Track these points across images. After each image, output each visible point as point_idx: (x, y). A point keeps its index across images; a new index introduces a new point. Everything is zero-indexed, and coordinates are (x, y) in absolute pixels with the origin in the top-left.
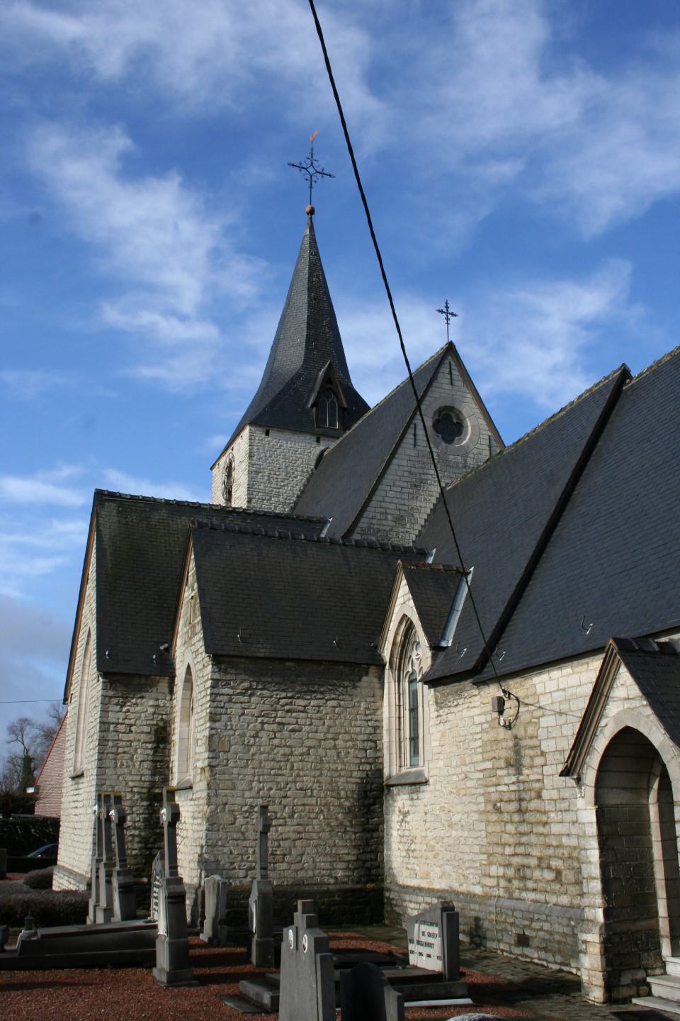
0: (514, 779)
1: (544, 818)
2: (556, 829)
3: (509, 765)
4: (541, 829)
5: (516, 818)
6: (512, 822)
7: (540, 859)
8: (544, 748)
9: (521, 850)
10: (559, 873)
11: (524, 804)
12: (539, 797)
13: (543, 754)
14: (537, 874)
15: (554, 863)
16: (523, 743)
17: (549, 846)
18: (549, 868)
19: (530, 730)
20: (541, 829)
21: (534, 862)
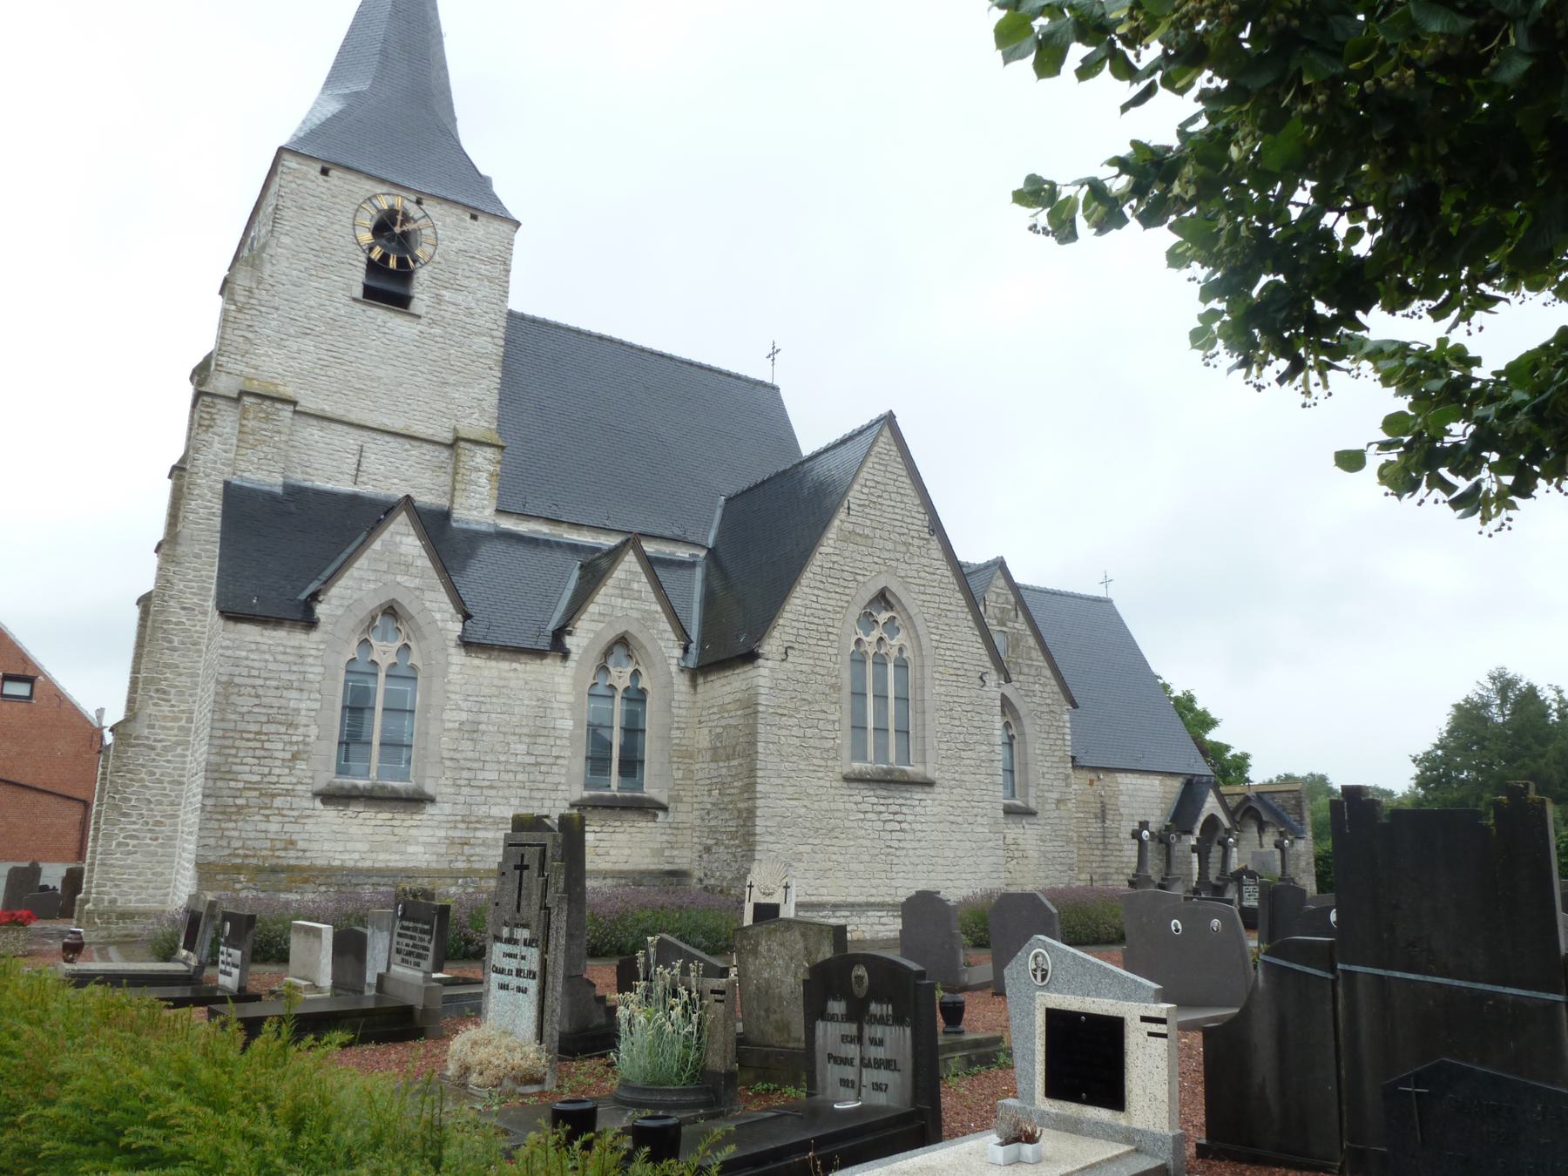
2: (1127, 853)
3: (1096, 817)
5: (1101, 847)
6: (1098, 849)
8: (1122, 810)
9: (1105, 864)
11: (1107, 840)
12: (1118, 837)
13: (1121, 815)
14: (1115, 877)
15: (1125, 871)
16: (1108, 807)
17: (1122, 862)
18: (1123, 873)
21: (1112, 871)
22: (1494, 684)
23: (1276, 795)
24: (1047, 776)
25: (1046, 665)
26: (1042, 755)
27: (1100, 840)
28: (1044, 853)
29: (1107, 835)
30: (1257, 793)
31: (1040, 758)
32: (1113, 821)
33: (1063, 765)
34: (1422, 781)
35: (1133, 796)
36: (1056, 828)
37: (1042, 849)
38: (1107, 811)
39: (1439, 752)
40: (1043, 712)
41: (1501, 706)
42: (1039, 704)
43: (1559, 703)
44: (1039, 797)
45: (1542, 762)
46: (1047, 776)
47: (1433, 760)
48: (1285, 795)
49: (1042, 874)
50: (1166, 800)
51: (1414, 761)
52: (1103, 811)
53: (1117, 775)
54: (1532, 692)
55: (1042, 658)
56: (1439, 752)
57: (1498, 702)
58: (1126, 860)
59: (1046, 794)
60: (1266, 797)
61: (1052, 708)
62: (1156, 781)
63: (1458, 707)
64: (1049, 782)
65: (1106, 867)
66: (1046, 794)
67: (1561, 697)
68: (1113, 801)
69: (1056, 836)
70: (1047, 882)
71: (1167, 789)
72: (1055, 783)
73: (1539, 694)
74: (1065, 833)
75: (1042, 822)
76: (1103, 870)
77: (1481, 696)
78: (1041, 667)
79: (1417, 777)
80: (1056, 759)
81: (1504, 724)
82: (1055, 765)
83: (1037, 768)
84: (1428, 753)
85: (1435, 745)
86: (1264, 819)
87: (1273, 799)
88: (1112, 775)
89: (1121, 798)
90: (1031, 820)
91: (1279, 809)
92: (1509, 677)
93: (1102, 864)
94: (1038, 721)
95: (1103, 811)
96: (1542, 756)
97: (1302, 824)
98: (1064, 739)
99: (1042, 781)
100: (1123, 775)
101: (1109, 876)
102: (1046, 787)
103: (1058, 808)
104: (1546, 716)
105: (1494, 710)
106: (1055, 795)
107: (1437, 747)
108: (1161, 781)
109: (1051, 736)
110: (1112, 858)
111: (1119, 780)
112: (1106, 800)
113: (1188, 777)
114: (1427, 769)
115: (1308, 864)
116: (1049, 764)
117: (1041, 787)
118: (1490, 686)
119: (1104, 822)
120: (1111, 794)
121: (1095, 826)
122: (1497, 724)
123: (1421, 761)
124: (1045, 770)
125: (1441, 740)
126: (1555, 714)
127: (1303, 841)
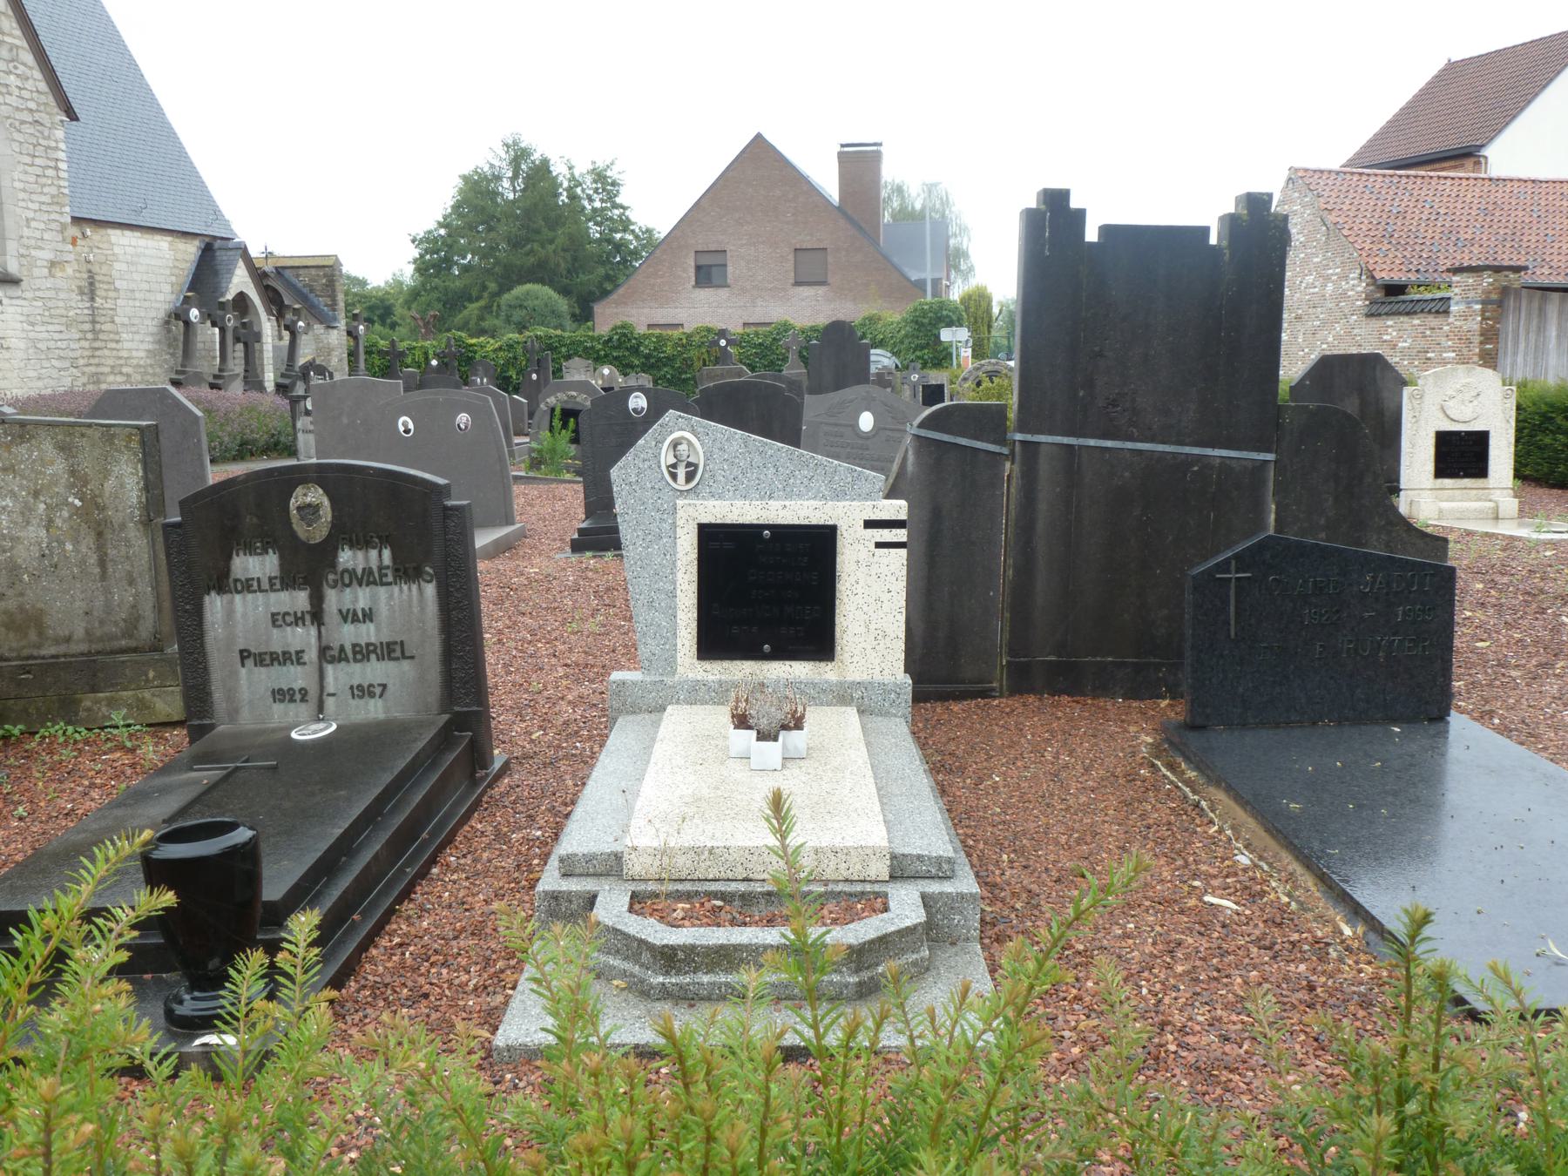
0: (88, 305)
1: (117, 338)
2: (126, 345)
4: (113, 345)
5: (89, 336)
6: (86, 339)
7: (113, 367)
8: (118, 284)
10: (128, 375)
11: (98, 326)
12: (113, 322)
13: (116, 290)
14: (111, 378)
15: (124, 370)
16: (97, 278)
17: (120, 358)
18: (121, 373)
19: (105, 269)
20: (113, 345)
21: (107, 370)
22: (507, 152)
23: (301, 272)
24: (33, 224)
25: (25, 45)
26: (24, 190)
27: (88, 327)
28: (34, 342)
29: (97, 319)
30: (276, 268)
31: (22, 195)
32: (106, 298)
33: (57, 208)
34: (422, 267)
35: (133, 263)
36: (50, 304)
37: (32, 335)
38: (97, 285)
39: (442, 232)
40: (23, 122)
41: (513, 179)
42: (17, 109)
43: (570, 181)
44: (22, 256)
45: (551, 248)
46: (33, 224)
47: (435, 240)
48: (313, 272)
49: (32, 374)
50: (177, 271)
51: (413, 241)
52: (91, 284)
53: (110, 231)
54: (543, 169)
55: (18, 33)
56: (442, 232)
57: (510, 174)
58: (125, 354)
59: (33, 253)
60: (287, 273)
61: (37, 116)
62: (164, 243)
63: (465, 178)
64: (38, 234)
65: (98, 365)
66: (33, 253)
67: (572, 174)
68: (105, 269)
69: (51, 316)
70: (40, 384)
71: (179, 256)
72: (46, 236)
73: (552, 168)
74: (64, 312)
75: (28, 295)
76: (93, 369)
77: (492, 166)
78: (17, 47)
79: (415, 261)
80: (46, 199)
81: (514, 201)
82: (44, 208)
83: (18, 211)
84: (430, 232)
85: (439, 223)
86: (286, 302)
87: (298, 276)
88: (102, 232)
89: (117, 266)
90: (13, 291)
91: (306, 290)
92: (523, 145)
93: (92, 361)
94: (16, 136)
95: (91, 284)
96: (551, 241)
97: (334, 310)
98: (57, 169)
99: (26, 232)
100: (118, 232)
101: (102, 378)
102: (33, 242)
103: (52, 275)
104: (557, 195)
105: (506, 184)
106: (47, 255)
107: (441, 225)
108: (170, 243)
109: (38, 161)
110: (106, 352)
111: (113, 239)
112: (96, 269)
113: (207, 240)
114: (427, 251)
115: (340, 360)
116: (36, 206)
117: (25, 241)
118: (504, 155)
119: (92, 299)
120: (103, 259)
121: (80, 306)
122: (507, 201)
123: (421, 241)
124: (31, 215)
125: (445, 217)
126: (565, 193)
127: (335, 332)
